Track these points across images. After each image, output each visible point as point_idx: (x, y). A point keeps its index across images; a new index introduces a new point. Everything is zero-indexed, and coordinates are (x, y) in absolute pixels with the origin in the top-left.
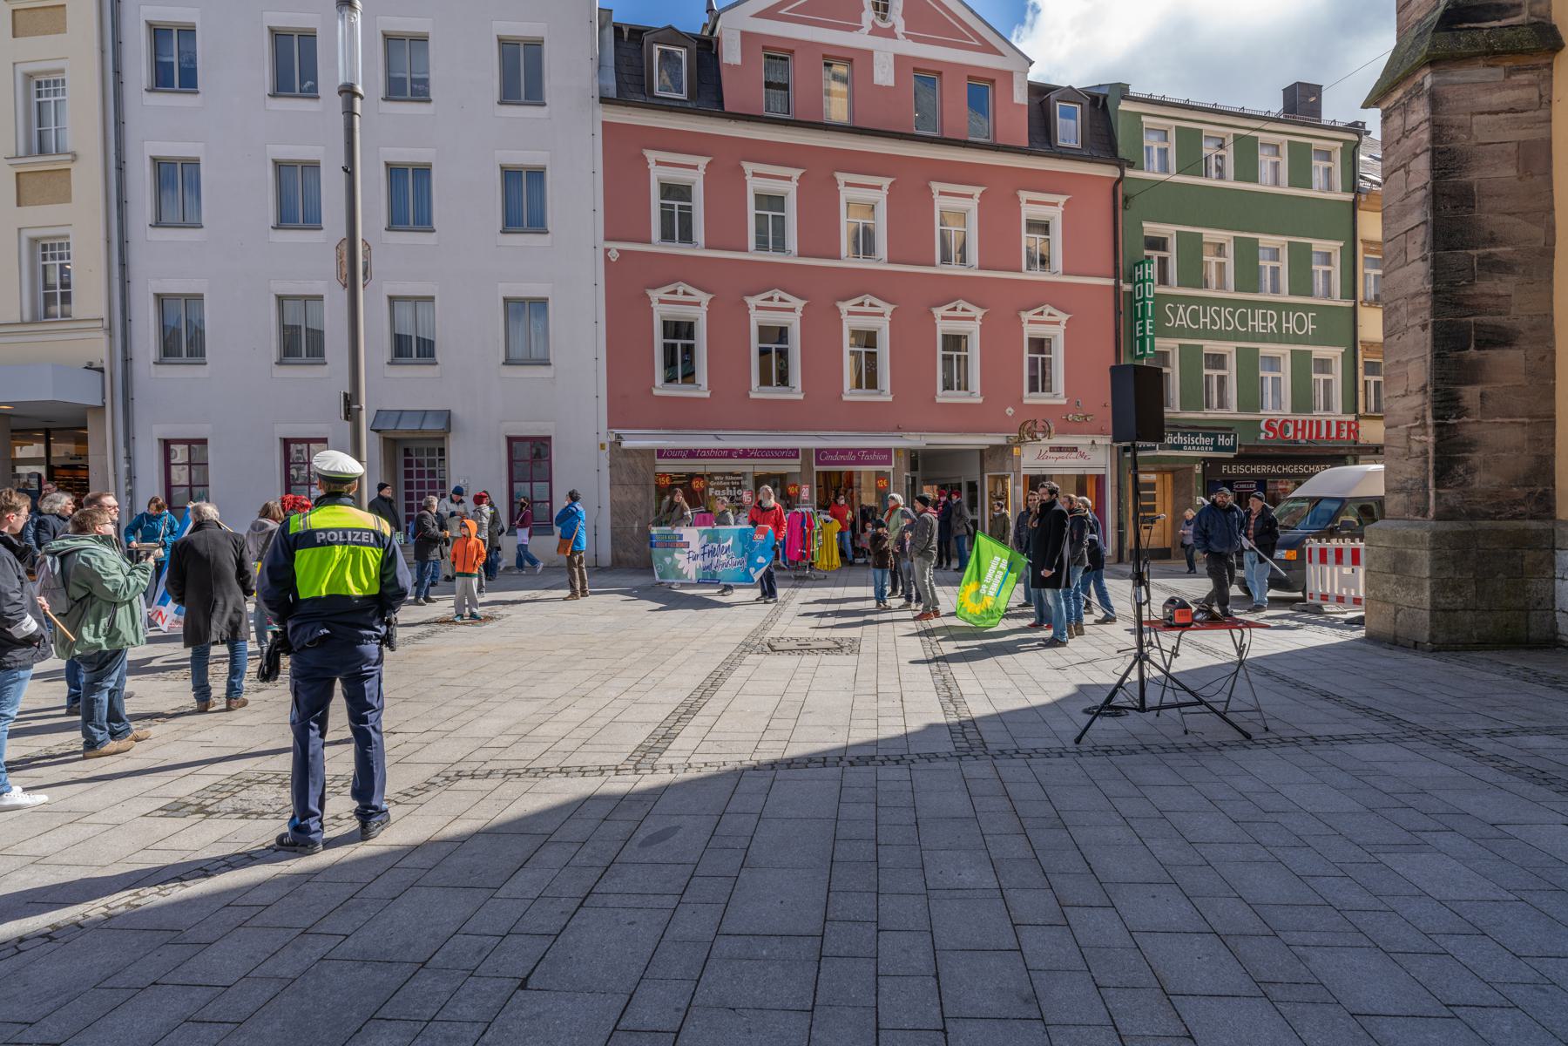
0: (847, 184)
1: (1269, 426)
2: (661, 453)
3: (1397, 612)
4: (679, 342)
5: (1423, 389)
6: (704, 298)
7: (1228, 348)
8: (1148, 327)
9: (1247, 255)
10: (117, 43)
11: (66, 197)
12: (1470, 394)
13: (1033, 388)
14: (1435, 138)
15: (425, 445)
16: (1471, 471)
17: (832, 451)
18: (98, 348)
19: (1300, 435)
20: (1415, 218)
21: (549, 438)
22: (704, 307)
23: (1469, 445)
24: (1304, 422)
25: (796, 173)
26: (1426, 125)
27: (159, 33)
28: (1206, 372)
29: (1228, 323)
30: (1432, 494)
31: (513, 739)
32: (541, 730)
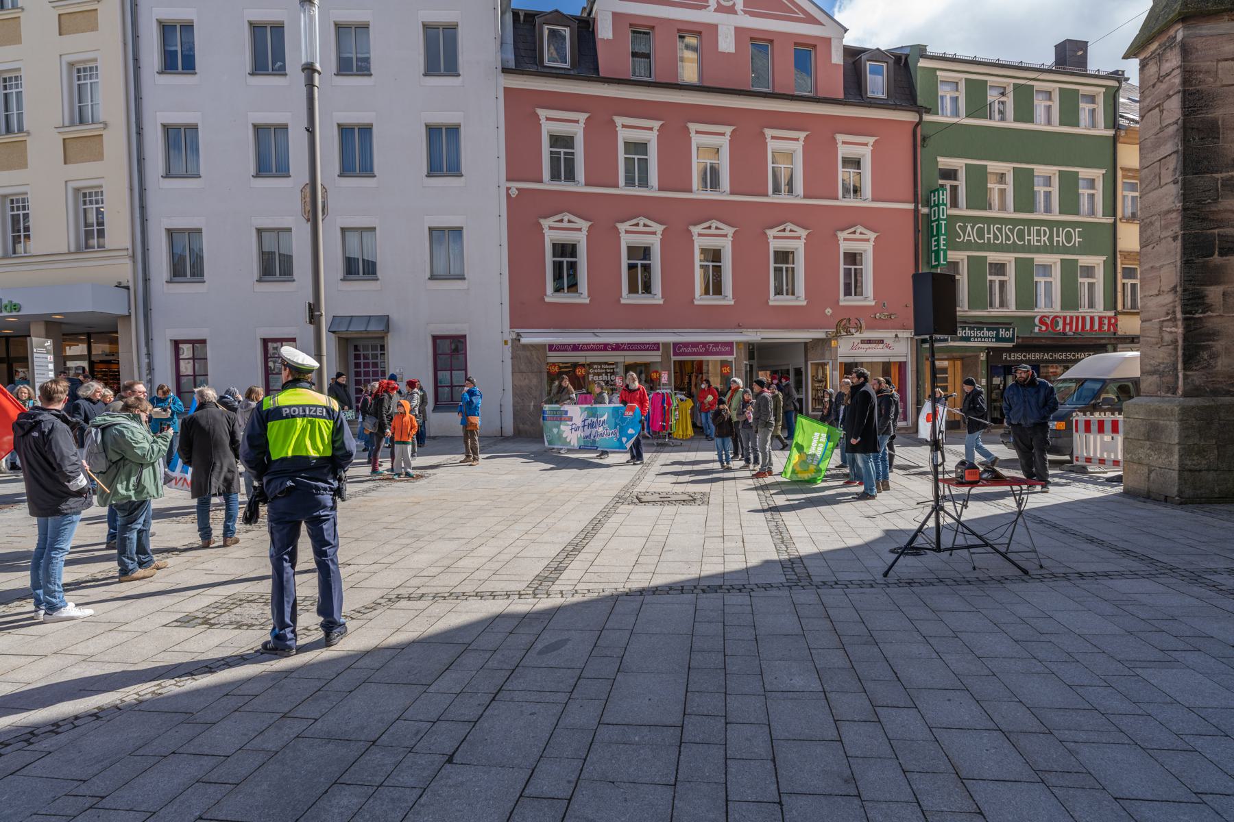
0: (697, 132)
1: (1042, 321)
2: (552, 347)
3: (1150, 472)
4: (565, 260)
5: (1174, 289)
6: (585, 225)
7: (1008, 258)
8: (942, 242)
9: (1024, 182)
10: (136, 37)
11: (99, 156)
12: (1214, 293)
13: (848, 292)
14: (1185, 82)
15: (370, 343)
16: (1214, 356)
17: (686, 345)
18: (125, 271)
19: (1068, 328)
20: (1169, 148)
21: (464, 337)
22: (585, 232)
23: (1213, 335)
24: (1071, 318)
25: (657, 124)
26: (1178, 71)
27: (166, 29)
28: (989, 278)
29: (1008, 238)
30: (1180, 375)
31: (439, 570)
32: (461, 563)
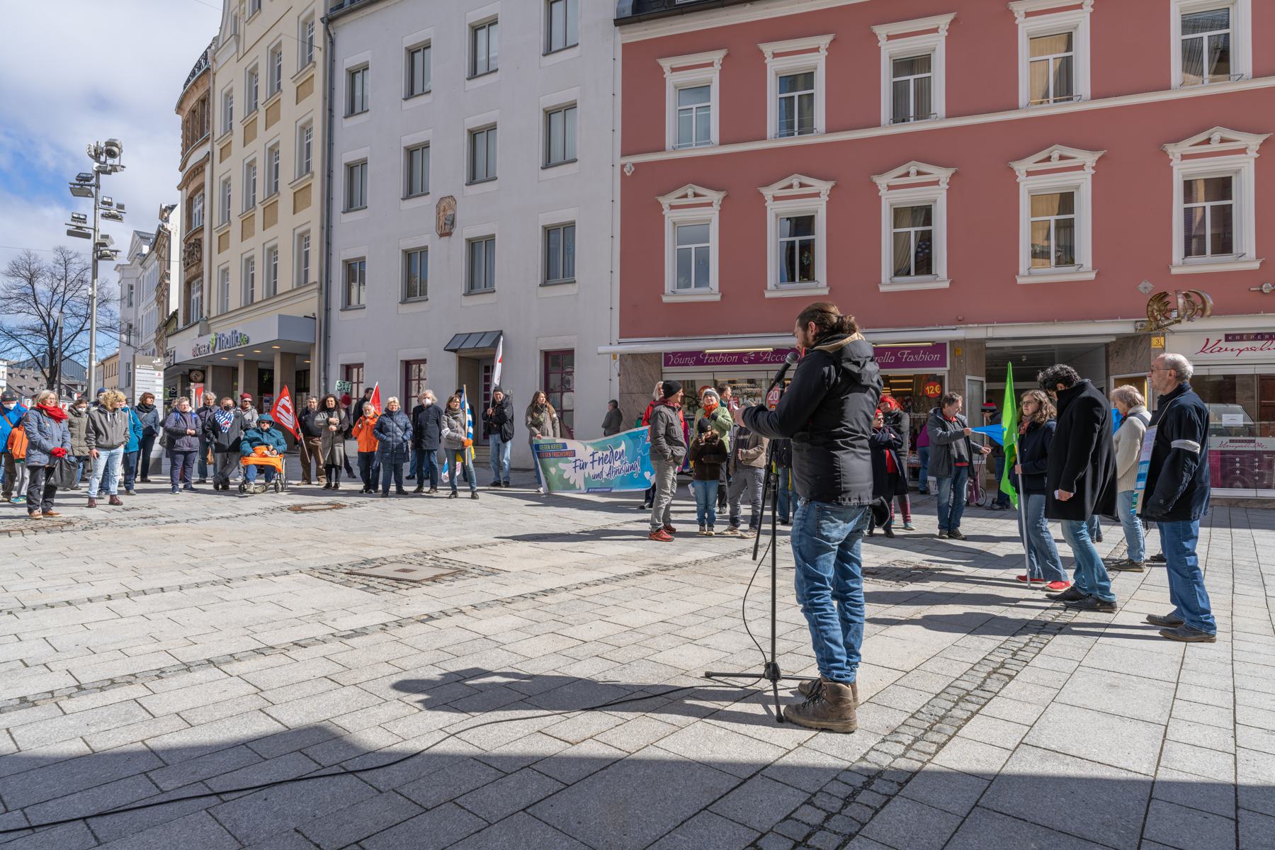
2: (672, 359)
18: (309, 304)
21: (570, 353)
